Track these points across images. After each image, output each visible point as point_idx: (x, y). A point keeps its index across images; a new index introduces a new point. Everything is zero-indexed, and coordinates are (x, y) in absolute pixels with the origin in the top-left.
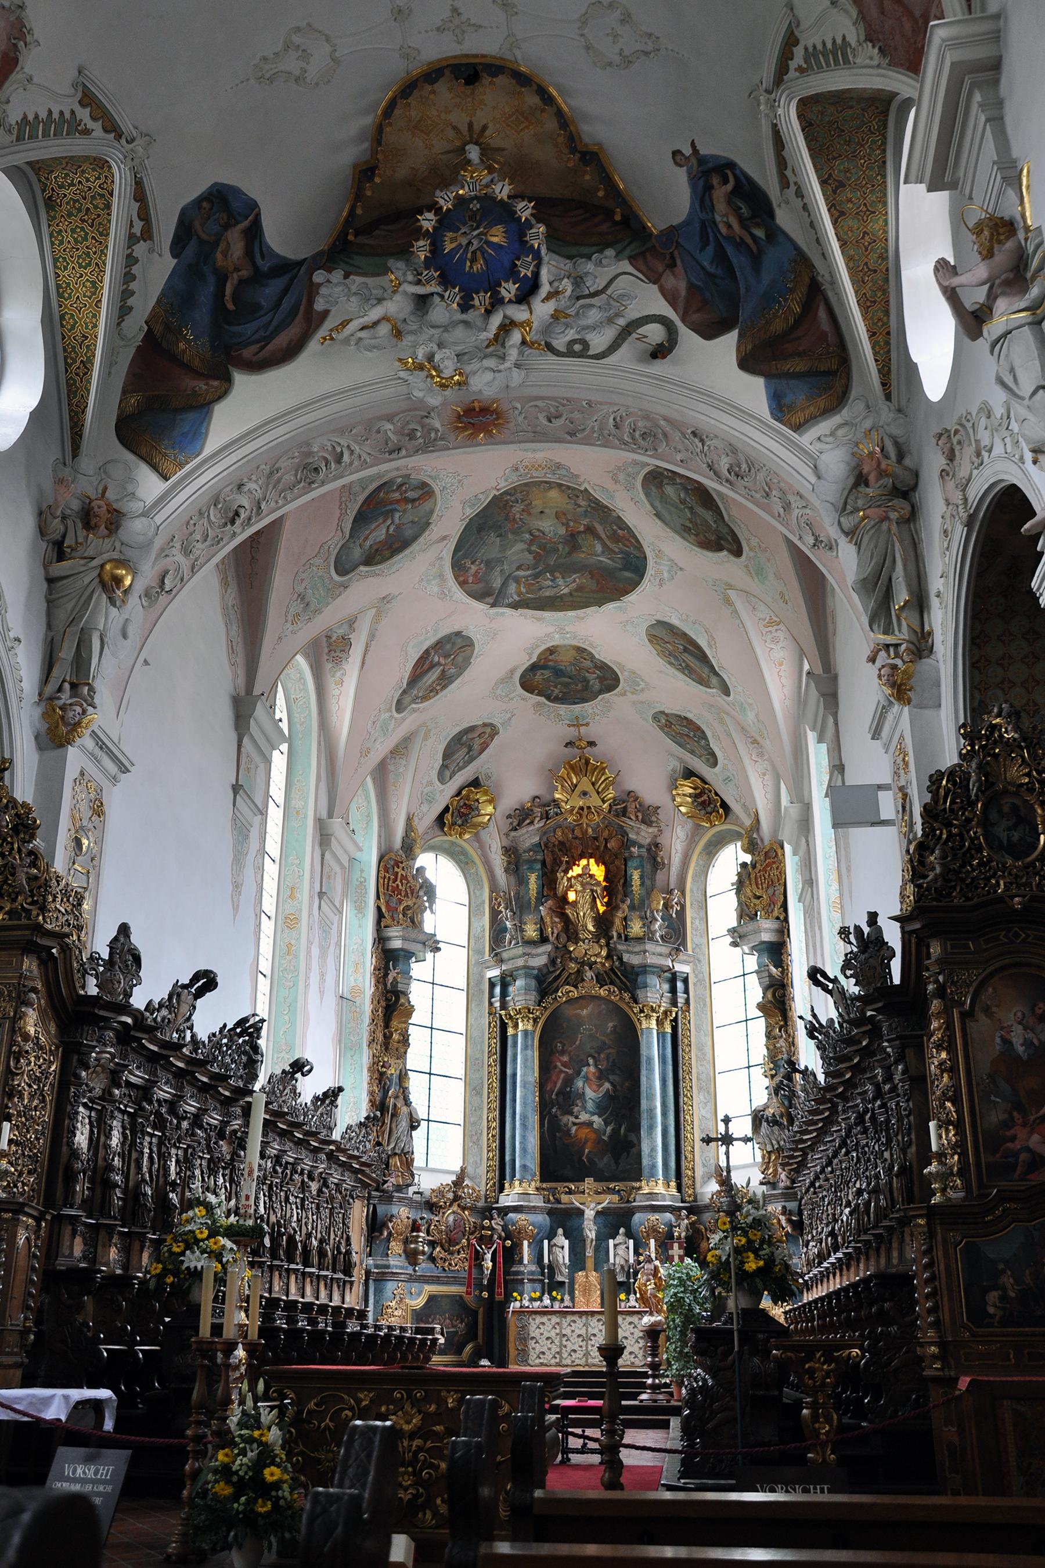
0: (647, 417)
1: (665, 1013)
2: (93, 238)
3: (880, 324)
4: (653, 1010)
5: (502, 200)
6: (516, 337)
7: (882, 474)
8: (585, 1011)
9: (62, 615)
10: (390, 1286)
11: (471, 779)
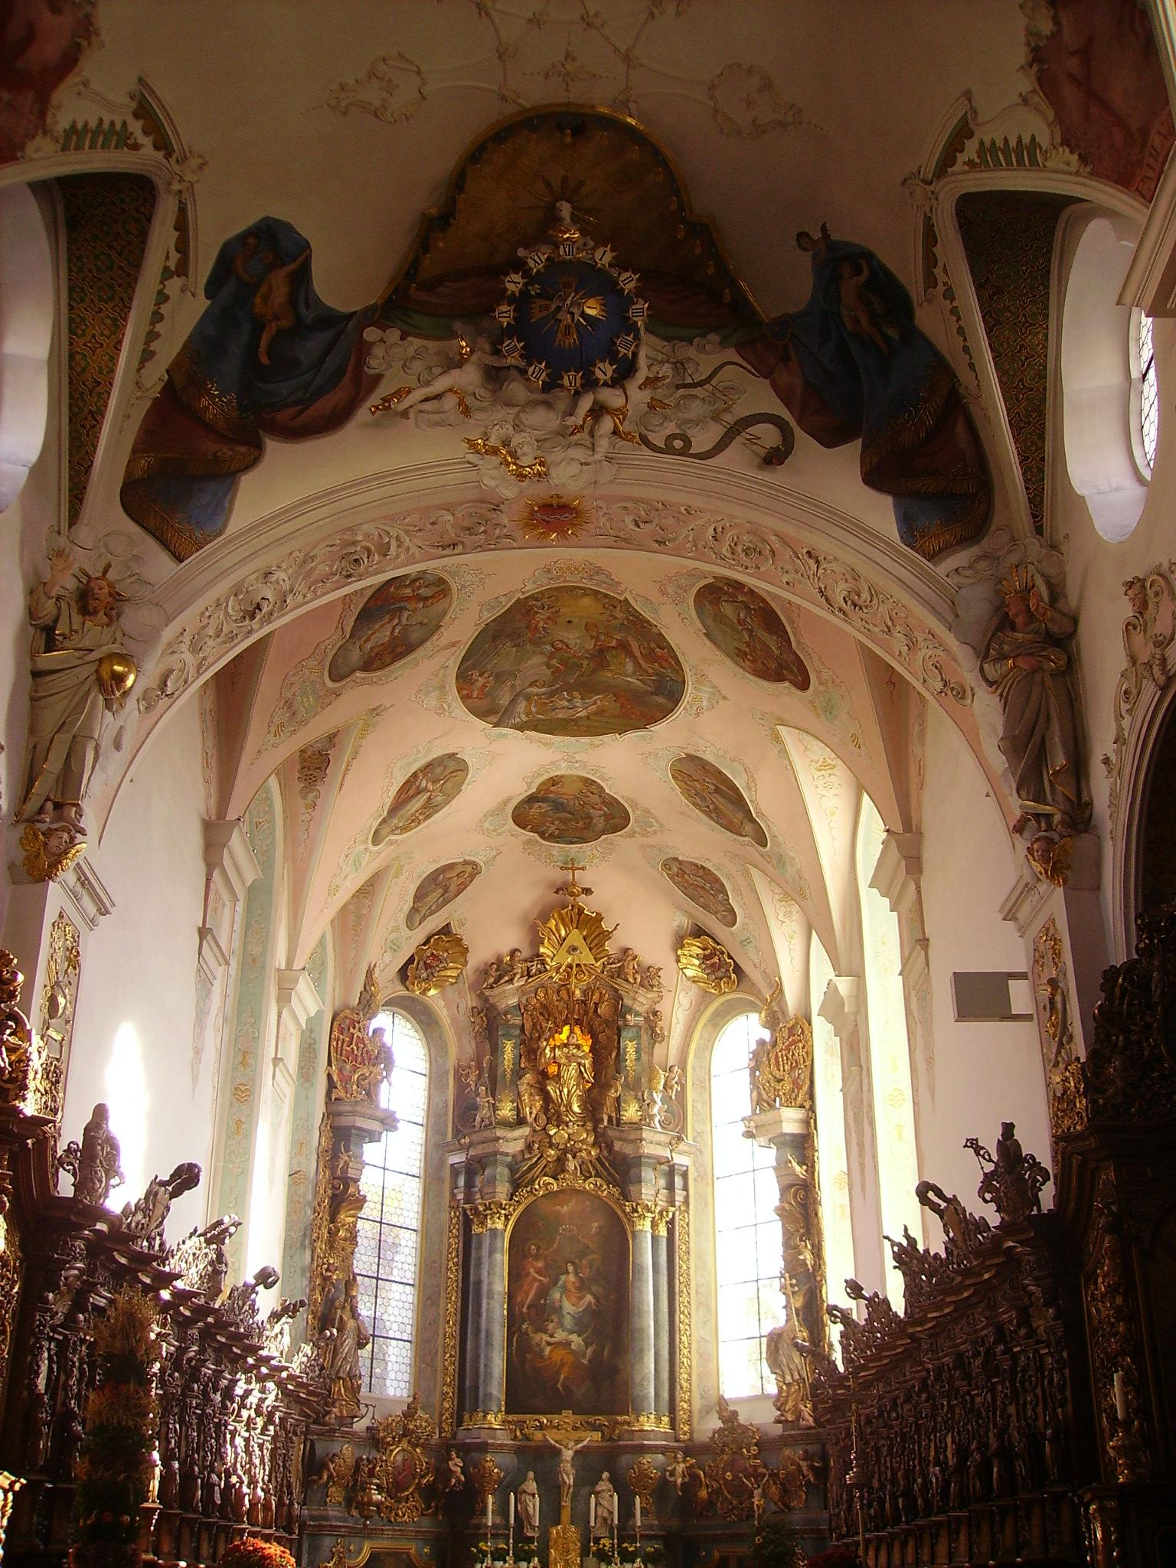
1: (661, 1213)
2: (121, 268)
3: (1033, 448)
4: (649, 1211)
6: (607, 424)
7: (1030, 617)
9: (49, 720)
10: (327, 1542)
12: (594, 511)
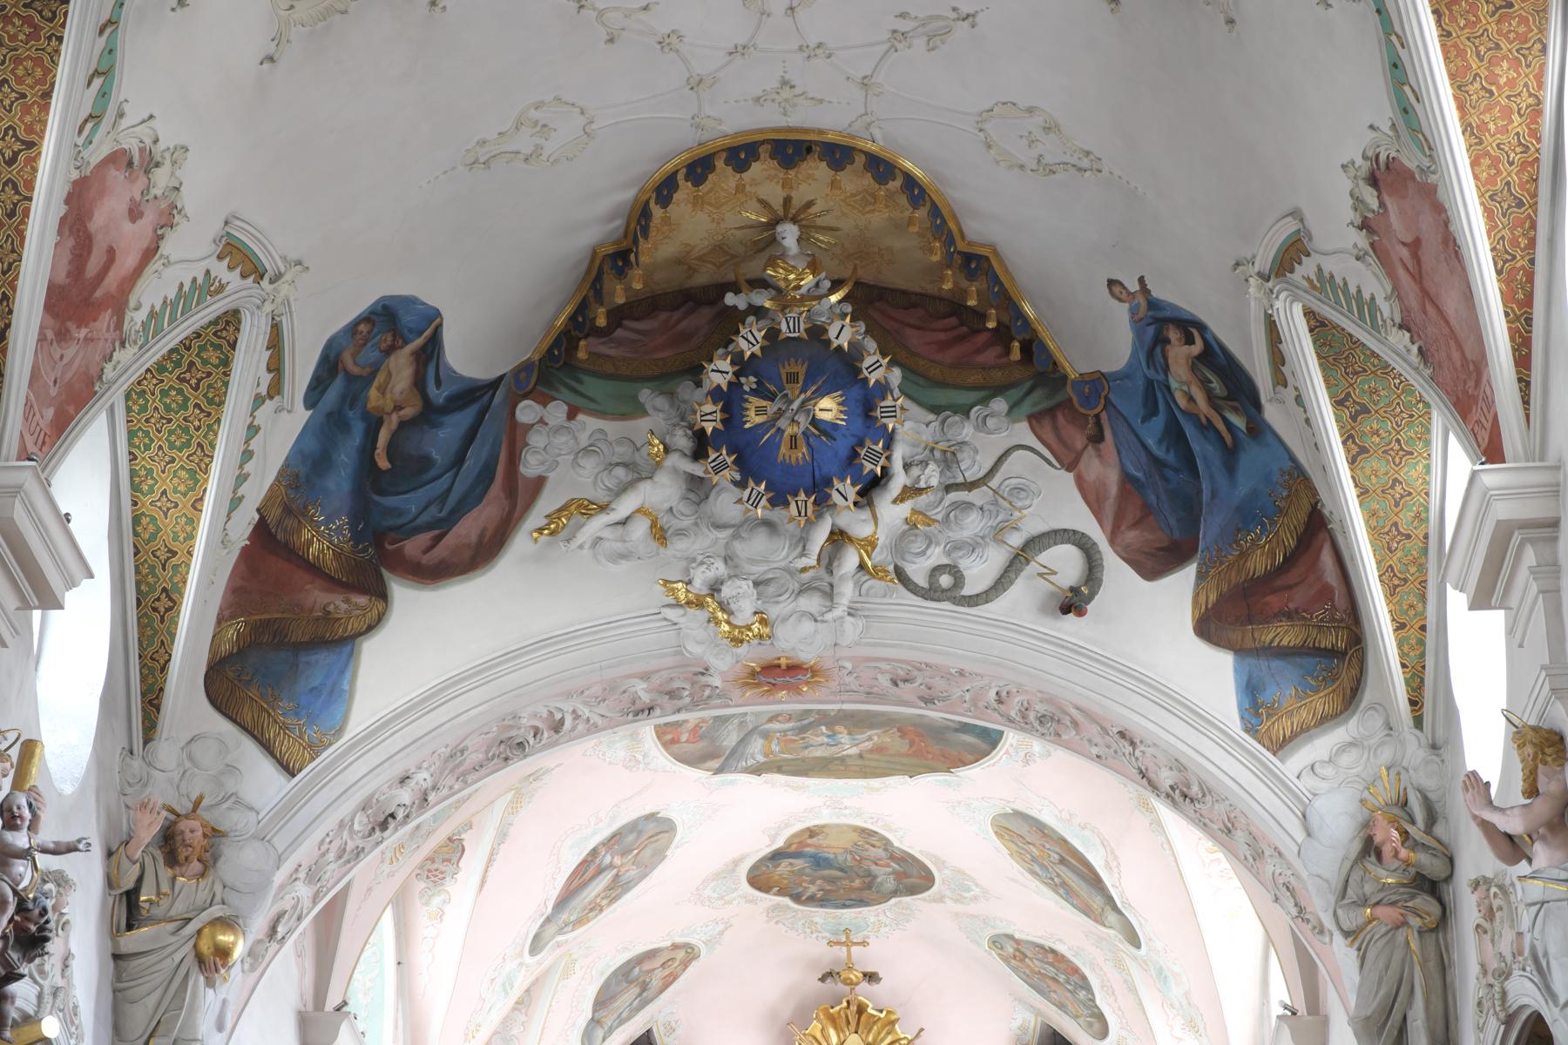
0: (1049, 700)
2: (197, 406)
5: (840, 348)
6: (850, 559)
11: (639, 1033)
12: (836, 670)
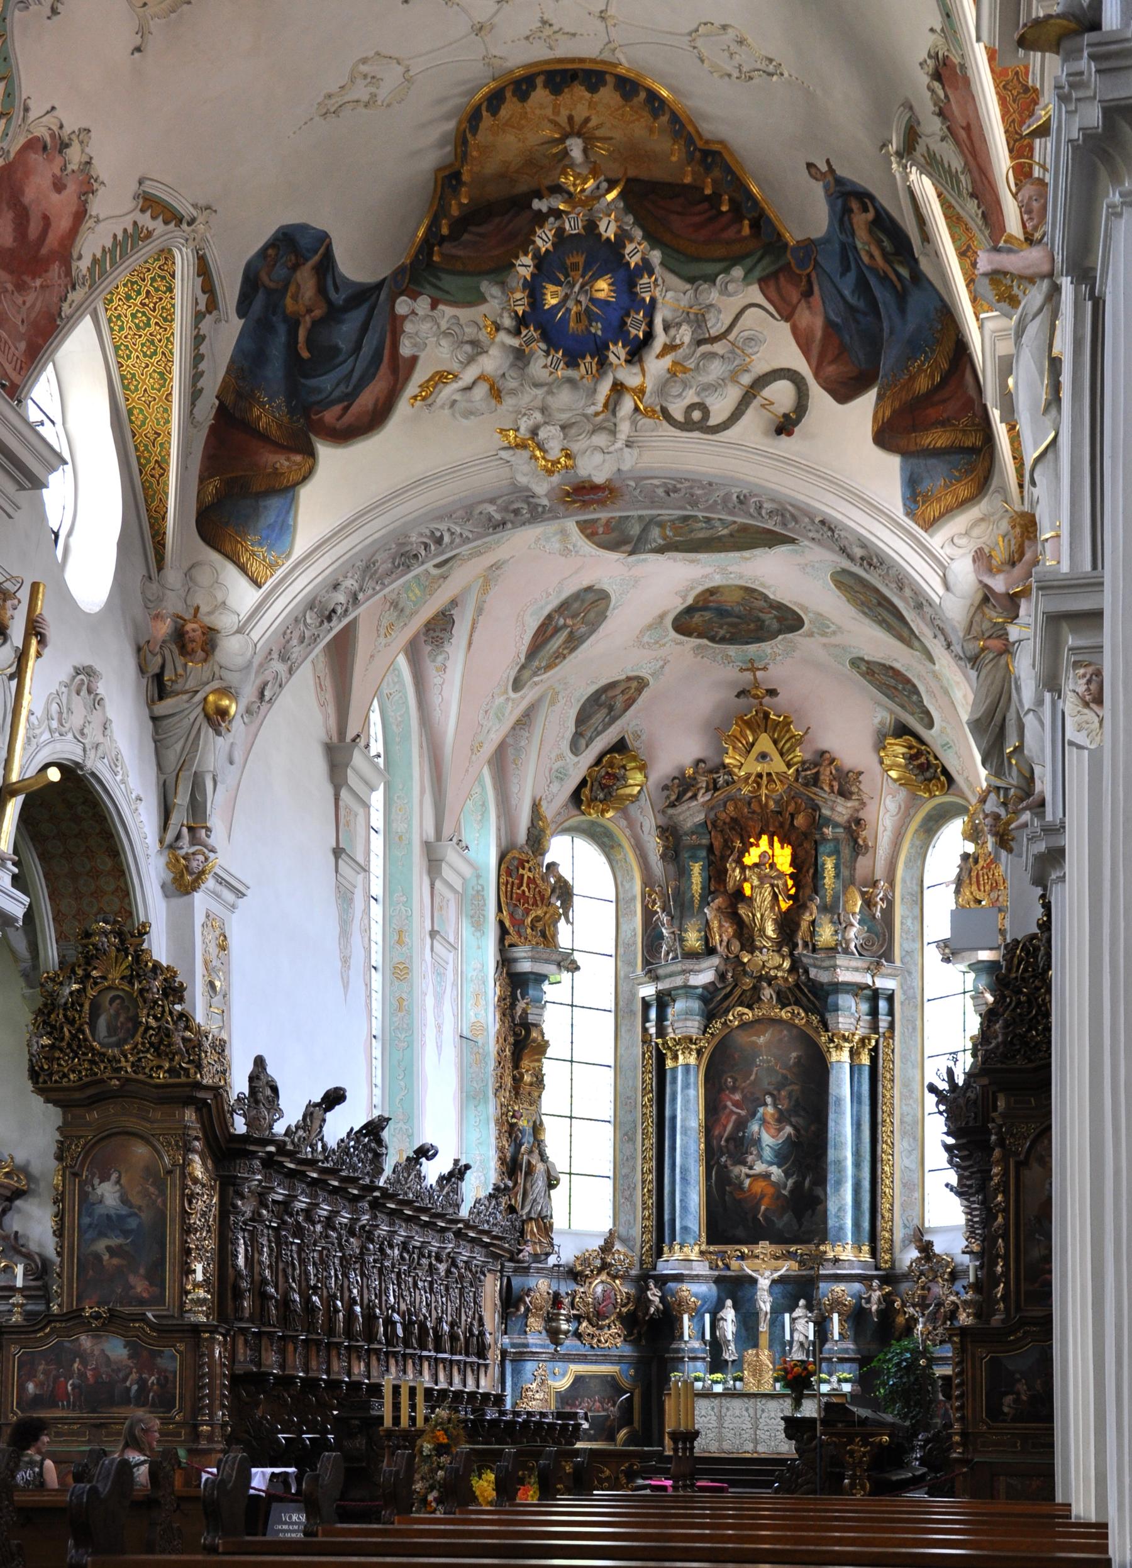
1: (863, 1041)
8: (762, 1040)
11: (615, 740)
